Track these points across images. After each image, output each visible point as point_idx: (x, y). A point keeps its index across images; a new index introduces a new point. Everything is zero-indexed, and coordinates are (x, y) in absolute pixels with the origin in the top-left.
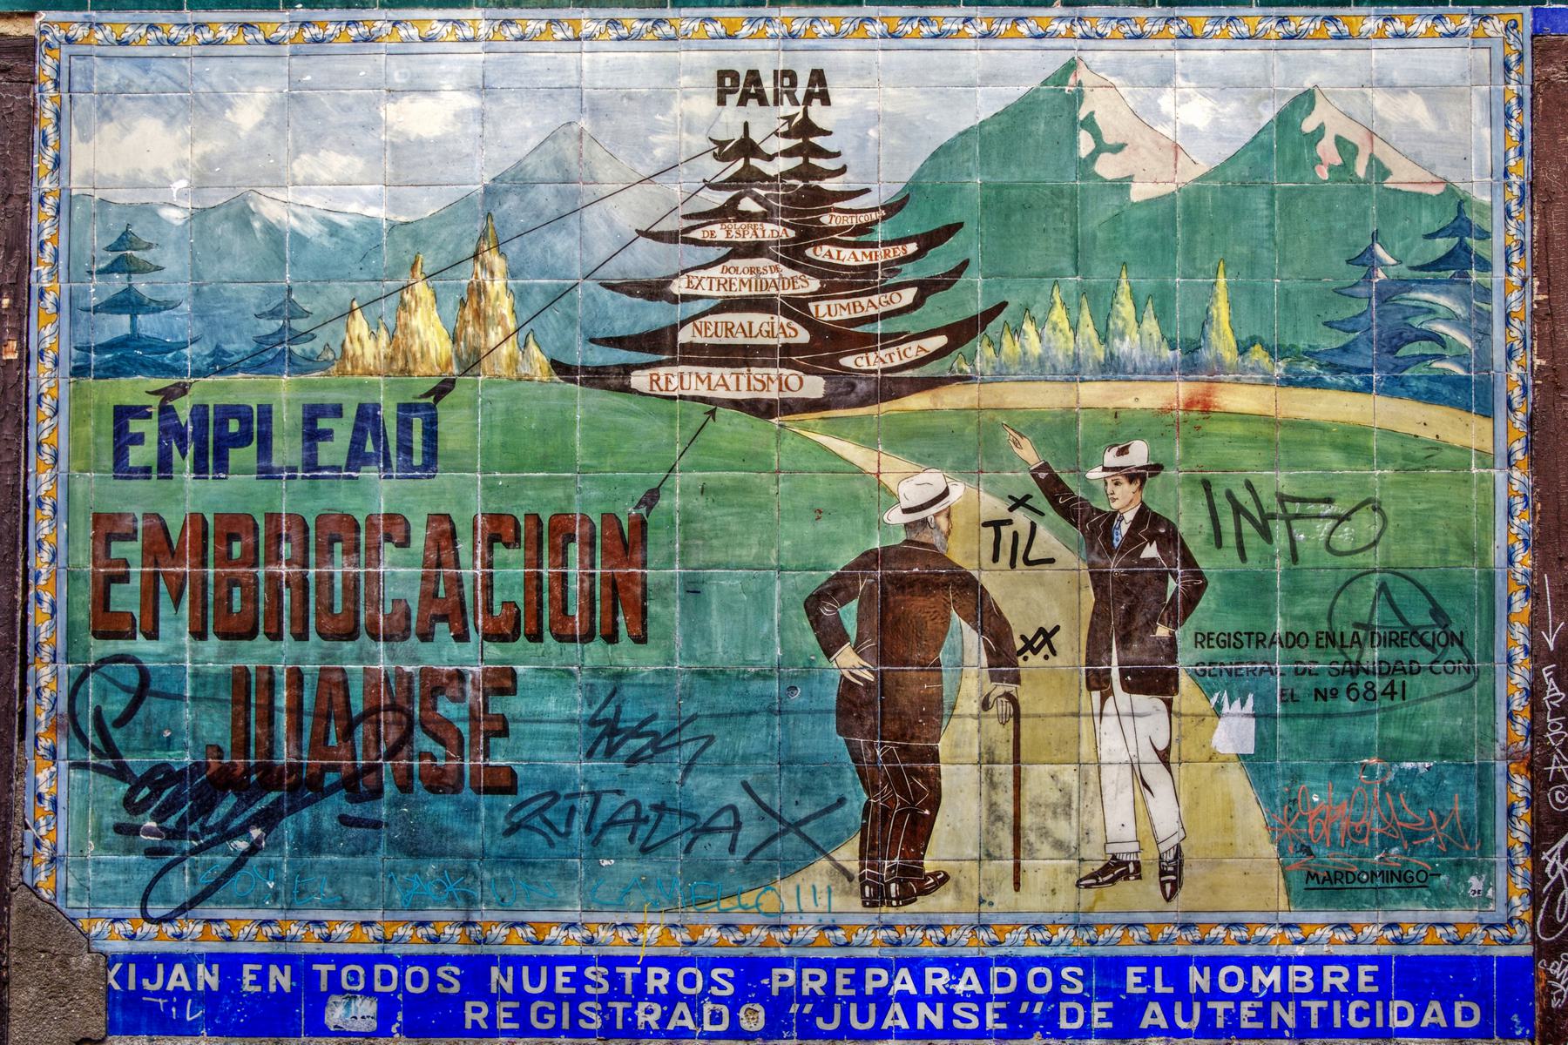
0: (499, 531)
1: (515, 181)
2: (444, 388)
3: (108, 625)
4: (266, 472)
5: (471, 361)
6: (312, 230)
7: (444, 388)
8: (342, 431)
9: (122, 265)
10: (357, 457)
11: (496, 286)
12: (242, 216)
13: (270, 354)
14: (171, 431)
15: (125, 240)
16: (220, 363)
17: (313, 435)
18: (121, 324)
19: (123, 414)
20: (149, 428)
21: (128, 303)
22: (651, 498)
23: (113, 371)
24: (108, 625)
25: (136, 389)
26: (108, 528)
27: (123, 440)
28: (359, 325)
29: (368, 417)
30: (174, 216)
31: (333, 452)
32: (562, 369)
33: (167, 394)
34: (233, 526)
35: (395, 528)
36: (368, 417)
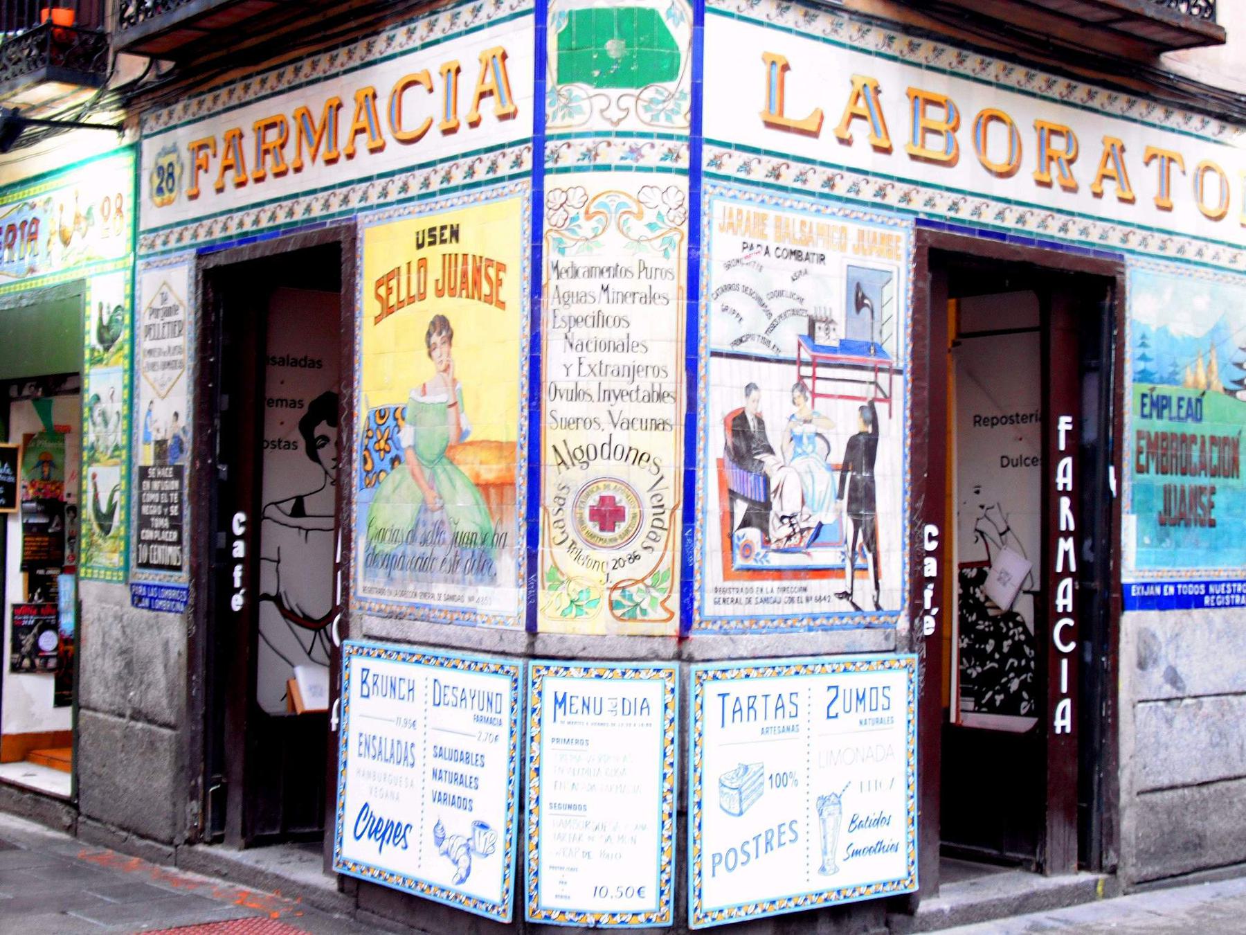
0: (1213, 440)
1: (1216, 330)
2: (1203, 394)
3: (1140, 469)
4: (1171, 419)
5: (1209, 385)
6: (1179, 338)
7: (1203, 394)
8: (1184, 404)
9: (1143, 345)
10: (1188, 416)
11: (1214, 362)
12: (1166, 332)
13: (1171, 380)
14: (1153, 404)
15: (1143, 337)
16: (1162, 381)
17: (1180, 407)
18: (1141, 365)
19: (1144, 396)
20: (1147, 401)
21: (1143, 358)
22: (1240, 433)
23: (1141, 380)
24: (1140, 469)
25: (1145, 387)
26: (1140, 435)
27: (1143, 405)
28: (1188, 370)
29: (1190, 401)
30: (1153, 329)
31: (1183, 413)
32: (1225, 390)
33: (1153, 389)
34: (1164, 436)
35: (1194, 438)
36: (1190, 401)
